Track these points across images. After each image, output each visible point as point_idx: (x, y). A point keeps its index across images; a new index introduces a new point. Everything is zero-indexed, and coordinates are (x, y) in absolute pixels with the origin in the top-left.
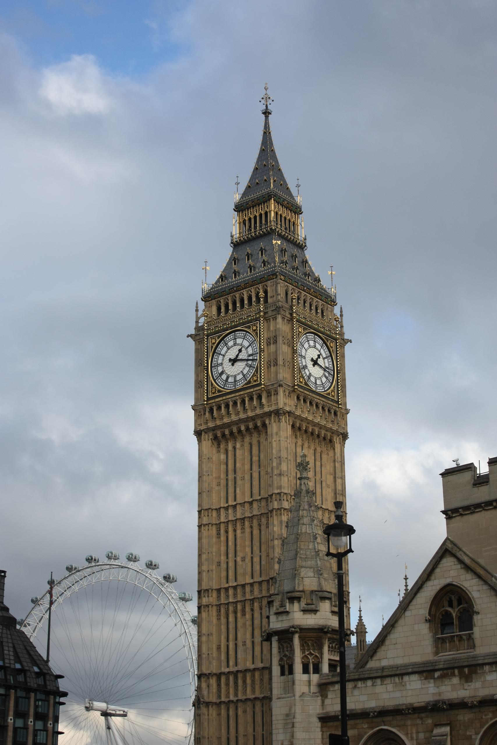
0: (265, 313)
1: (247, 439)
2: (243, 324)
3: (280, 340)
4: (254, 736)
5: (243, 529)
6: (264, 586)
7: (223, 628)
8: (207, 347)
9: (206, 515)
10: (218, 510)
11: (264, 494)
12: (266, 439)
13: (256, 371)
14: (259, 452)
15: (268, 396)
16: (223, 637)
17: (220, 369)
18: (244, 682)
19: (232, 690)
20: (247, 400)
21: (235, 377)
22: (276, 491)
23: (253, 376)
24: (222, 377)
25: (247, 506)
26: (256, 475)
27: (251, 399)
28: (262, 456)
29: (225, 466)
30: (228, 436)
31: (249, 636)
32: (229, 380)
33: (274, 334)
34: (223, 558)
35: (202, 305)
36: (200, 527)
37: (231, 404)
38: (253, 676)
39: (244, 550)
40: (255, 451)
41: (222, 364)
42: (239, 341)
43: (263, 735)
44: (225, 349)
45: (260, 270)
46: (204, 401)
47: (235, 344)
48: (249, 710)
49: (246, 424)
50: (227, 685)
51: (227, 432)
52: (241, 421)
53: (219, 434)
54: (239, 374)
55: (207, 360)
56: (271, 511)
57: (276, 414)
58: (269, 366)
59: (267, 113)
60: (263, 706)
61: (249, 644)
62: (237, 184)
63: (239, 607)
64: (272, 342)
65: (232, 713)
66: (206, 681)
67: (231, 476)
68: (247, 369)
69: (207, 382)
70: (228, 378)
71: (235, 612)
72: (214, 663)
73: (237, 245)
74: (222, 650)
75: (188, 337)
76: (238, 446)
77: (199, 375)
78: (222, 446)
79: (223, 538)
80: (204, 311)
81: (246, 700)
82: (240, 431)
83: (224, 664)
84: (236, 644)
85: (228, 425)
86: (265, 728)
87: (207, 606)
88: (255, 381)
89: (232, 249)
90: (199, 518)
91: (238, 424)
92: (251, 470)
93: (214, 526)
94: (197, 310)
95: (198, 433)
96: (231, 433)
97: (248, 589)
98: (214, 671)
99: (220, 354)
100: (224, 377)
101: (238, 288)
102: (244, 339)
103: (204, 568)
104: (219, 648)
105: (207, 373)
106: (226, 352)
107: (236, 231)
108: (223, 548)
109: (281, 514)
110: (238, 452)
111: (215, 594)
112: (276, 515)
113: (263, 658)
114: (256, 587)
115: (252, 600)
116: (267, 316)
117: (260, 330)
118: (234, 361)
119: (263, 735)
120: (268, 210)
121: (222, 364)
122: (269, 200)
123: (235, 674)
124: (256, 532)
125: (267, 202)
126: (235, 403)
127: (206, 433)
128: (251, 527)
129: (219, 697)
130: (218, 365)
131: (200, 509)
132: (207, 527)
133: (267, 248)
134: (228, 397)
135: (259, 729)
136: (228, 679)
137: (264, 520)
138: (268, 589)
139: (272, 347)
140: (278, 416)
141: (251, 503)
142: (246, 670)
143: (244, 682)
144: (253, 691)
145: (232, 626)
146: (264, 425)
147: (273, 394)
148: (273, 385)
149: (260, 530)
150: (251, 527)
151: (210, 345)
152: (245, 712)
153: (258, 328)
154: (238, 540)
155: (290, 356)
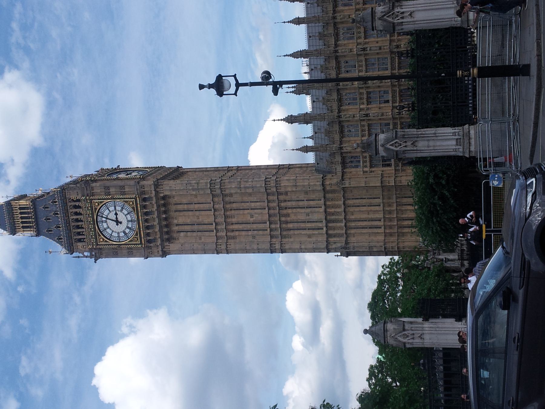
1: (172, 214)
2: (93, 214)
5: (232, 217)
6: (271, 198)
7: (296, 232)
8: (105, 245)
9: (220, 246)
10: (218, 238)
11: (209, 199)
17: (122, 234)
18: (333, 214)
19: (338, 225)
21: (128, 221)
22: (209, 186)
24: (127, 232)
25: (216, 213)
27: (145, 207)
28: (184, 201)
29: (189, 233)
31: (303, 210)
32: (130, 226)
34: (250, 233)
35: (75, 254)
36: (228, 252)
40: (180, 207)
41: (118, 233)
44: (108, 230)
47: (106, 222)
48: (351, 209)
50: (334, 229)
51: (165, 230)
52: (158, 217)
53: (166, 237)
54: (127, 218)
55: (114, 245)
57: (157, 187)
58: (124, 193)
61: (309, 210)
63: (283, 219)
65: (353, 224)
66: (332, 245)
67: (196, 227)
69: (129, 244)
70: (128, 227)
71: (287, 222)
72: (320, 239)
76: (176, 221)
78: (175, 235)
79: (237, 233)
81: (345, 211)
82: (166, 219)
83: (320, 231)
84: (308, 222)
85: (161, 228)
86: (364, 197)
88: (133, 203)
94: (79, 257)
95: (164, 254)
96: (167, 226)
97: (272, 212)
98: (325, 239)
100: (127, 231)
101: (67, 223)
103: (255, 247)
104: (309, 236)
105: (123, 244)
107: (28, 233)
108: (244, 233)
109: (224, 183)
111: (274, 240)
113: (317, 198)
114: (271, 205)
115: (280, 208)
116: (89, 195)
118: (118, 222)
121: (118, 233)
123: (328, 221)
124: (234, 206)
126: (146, 221)
127: (164, 248)
128: (231, 210)
130: (119, 237)
132: (228, 246)
133: (45, 204)
137: (227, 199)
139: (112, 190)
141: (215, 210)
142: (325, 212)
144: (338, 206)
145: (296, 225)
146: (164, 198)
151: (103, 243)
153: (97, 201)
154: (240, 220)
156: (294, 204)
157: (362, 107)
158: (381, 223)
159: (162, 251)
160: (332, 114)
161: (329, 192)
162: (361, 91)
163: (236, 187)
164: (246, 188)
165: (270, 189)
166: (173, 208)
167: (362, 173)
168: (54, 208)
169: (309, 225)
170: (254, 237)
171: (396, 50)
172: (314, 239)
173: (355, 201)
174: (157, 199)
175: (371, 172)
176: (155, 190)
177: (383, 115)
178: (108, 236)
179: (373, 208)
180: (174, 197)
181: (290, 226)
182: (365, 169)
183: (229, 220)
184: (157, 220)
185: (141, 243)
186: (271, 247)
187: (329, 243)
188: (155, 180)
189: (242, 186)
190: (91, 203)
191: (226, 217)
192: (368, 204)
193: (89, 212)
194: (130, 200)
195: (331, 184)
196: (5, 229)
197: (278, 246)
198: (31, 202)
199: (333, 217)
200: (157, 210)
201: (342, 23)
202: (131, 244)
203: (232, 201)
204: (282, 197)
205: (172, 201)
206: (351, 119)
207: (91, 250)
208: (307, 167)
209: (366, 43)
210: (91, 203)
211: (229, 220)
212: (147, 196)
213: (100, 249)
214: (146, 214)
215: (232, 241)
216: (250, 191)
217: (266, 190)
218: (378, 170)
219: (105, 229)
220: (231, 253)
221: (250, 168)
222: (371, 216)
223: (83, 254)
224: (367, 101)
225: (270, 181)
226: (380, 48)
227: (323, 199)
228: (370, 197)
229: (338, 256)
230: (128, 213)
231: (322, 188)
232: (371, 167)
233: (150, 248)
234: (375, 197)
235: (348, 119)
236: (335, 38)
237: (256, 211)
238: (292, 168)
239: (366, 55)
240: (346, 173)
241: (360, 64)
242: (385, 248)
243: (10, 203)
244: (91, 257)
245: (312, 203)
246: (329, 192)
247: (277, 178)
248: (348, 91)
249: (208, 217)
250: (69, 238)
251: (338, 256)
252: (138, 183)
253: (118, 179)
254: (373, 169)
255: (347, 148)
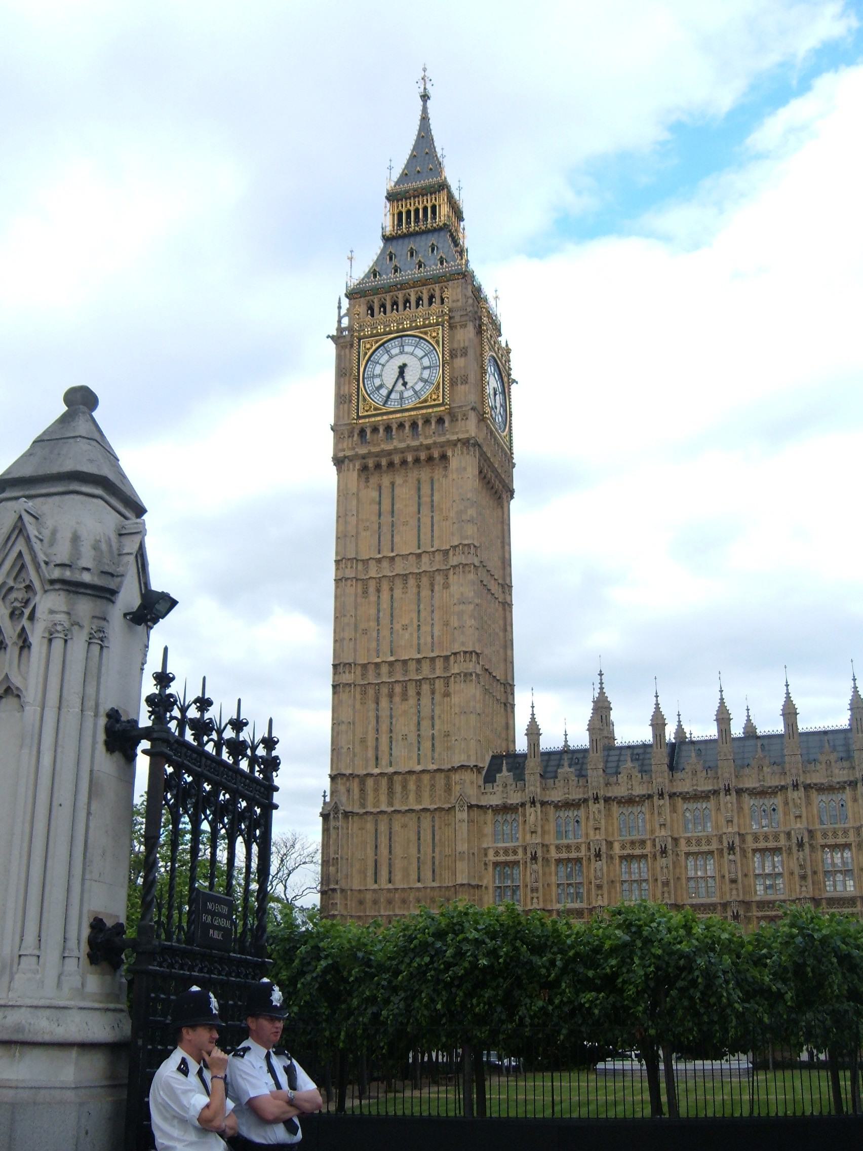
0: (450, 318)
1: (413, 475)
2: (417, 328)
3: (471, 352)
4: (419, 858)
6: (439, 664)
7: (372, 714)
8: (359, 352)
9: (349, 566)
10: (365, 562)
12: (446, 476)
13: (438, 388)
14: (432, 489)
15: (452, 421)
16: (370, 728)
18: (405, 787)
19: (383, 798)
20: (420, 423)
23: (431, 394)
26: (426, 520)
27: (427, 421)
30: (384, 468)
31: (413, 728)
33: (462, 345)
34: (373, 624)
35: (345, 303)
36: (337, 581)
37: (394, 426)
38: (419, 780)
39: (407, 615)
40: (426, 490)
41: (380, 376)
42: (408, 349)
43: (433, 857)
45: (433, 268)
46: (354, 419)
47: (402, 353)
49: (416, 453)
50: (376, 790)
51: (384, 462)
53: (371, 463)
56: (454, 567)
57: (464, 444)
58: (453, 383)
59: (425, 97)
60: (433, 821)
61: (413, 738)
62: (390, 168)
63: (398, 689)
64: (459, 355)
65: (383, 828)
66: (344, 784)
67: (386, 519)
68: (421, 384)
71: (391, 696)
73: (387, 239)
74: (369, 744)
75: (328, 337)
76: (399, 481)
77: (342, 388)
78: (374, 480)
79: (373, 598)
80: (348, 310)
82: (404, 462)
83: (372, 762)
84: (391, 737)
85: (389, 453)
86: (437, 850)
87: (350, 685)
88: (434, 400)
89: (382, 245)
90: (337, 569)
91: (403, 453)
92: (419, 512)
93: (360, 583)
94: (339, 308)
95: (338, 461)
96: (391, 464)
97: (412, 666)
98: (356, 772)
99: (378, 363)
101: (402, 286)
102: (416, 346)
104: (363, 741)
105: (358, 385)
106: (388, 361)
108: (373, 611)
110: (397, 491)
111: (359, 671)
112: (463, 572)
114: (426, 666)
115: (419, 683)
116: (452, 321)
117: (443, 337)
119: (433, 857)
120: (437, 203)
121: (380, 376)
122: (439, 192)
123: (390, 777)
124: (426, 593)
125: (435, 193)
127: (351, 460)
128: (419, 586)
129: (363, 805)
130: (374, 377)
131: (339, 558)
132: (349, 582)
133: (440, 246)
134: (391, 417)
135: (427, 849)
136: (377, 783)
137: (439, 579)
138: (446, 669)
139: (460, 362)
140: (468, 447)
141: (419, 556)
142: (411, 772)
143: (405, 787)
146: (444, 457)
147: (460, 418)
148: (460, 407)
149: (432, 591)
150: (419, 586)
152: (404, 826)
155: (479, 377)
156: (426, 711)
157: (617, 846)
158: (384, 884)
159: (345, 457)
160: (602, 785)
161: (448, 778)
162: (649, 843)
163: (462, 594)
164: (460, 614)
165: (455, 662)
166: (425, 474)
167: (485, 845)
168: (432, 262)
169: (384, 740)
170: (365, 632)
171: (730, 914)
172: (358, 749)
173: (429, 832)
174: (442, 445)
175: (486, 864)
176: (459, 440)
177: (599, 887)
178: (375, 357)
179: (415, 866)
180: (446, 476)
181: (384, 703)
182: (491, 853)
183: (399, 583)
184: (402, 445)
185: (359, 417)
186: (345, 664)
187: (348, 779)
188: (480, 441)
189: (462, 607)
190: (437, 324)
191: (405, 577)
192: (422, 858)
193: (420, 322)
194: (441, 394)
195: (462, 782)
196: (397, 183)
197: (347, 678)
198: (445, 224)
199: (398, 788)
200: (421, 445)
201: (786, 803)
202: (358, 399)
203: (436, 588)
204: (439, 684)
205: (438, 473)
206: (591, 823)
207: (350, 328)
208: (507, 740)
209: (743, 851)
210: (437, 324)
211: (399, 583)
212: (447, 424)
213: (352, 346)
214: (414, 425)
215: (360, 591)
216: (454, 622)
217: (455, 654)
218: (488, 879)
219: (387, 352)
220: (337, 587)
221: (508, 628)
222: (398, 864)
223: (345, 315)
224: (629, 856)
225: (471, 661)
226: (734, 881)
227: (435, 767)
228: (437, 863)
229: (324, 796)
230: (416, 392)
231: (456, 765)
232: (496, 864)
233: (351, 435)
234: (437, 871)
235: (591, 817)
236: (754, 788)
237: (415, 635)
238: (506, 710)
239: (721, 851)
240: (485, 813)
241: (703, 842)
242: (334, 890)
243: (443, 189)
244: (340, 329)
245: (427, 744)
246: (448, 778)
247: (478, 675)
248: (647, 816)
249: (406, 543)
250: (375, 291)
251: (324, 796)
252: (473, 409)
253: (483, 372)
254: (490, 868)
255: (533, 815)
